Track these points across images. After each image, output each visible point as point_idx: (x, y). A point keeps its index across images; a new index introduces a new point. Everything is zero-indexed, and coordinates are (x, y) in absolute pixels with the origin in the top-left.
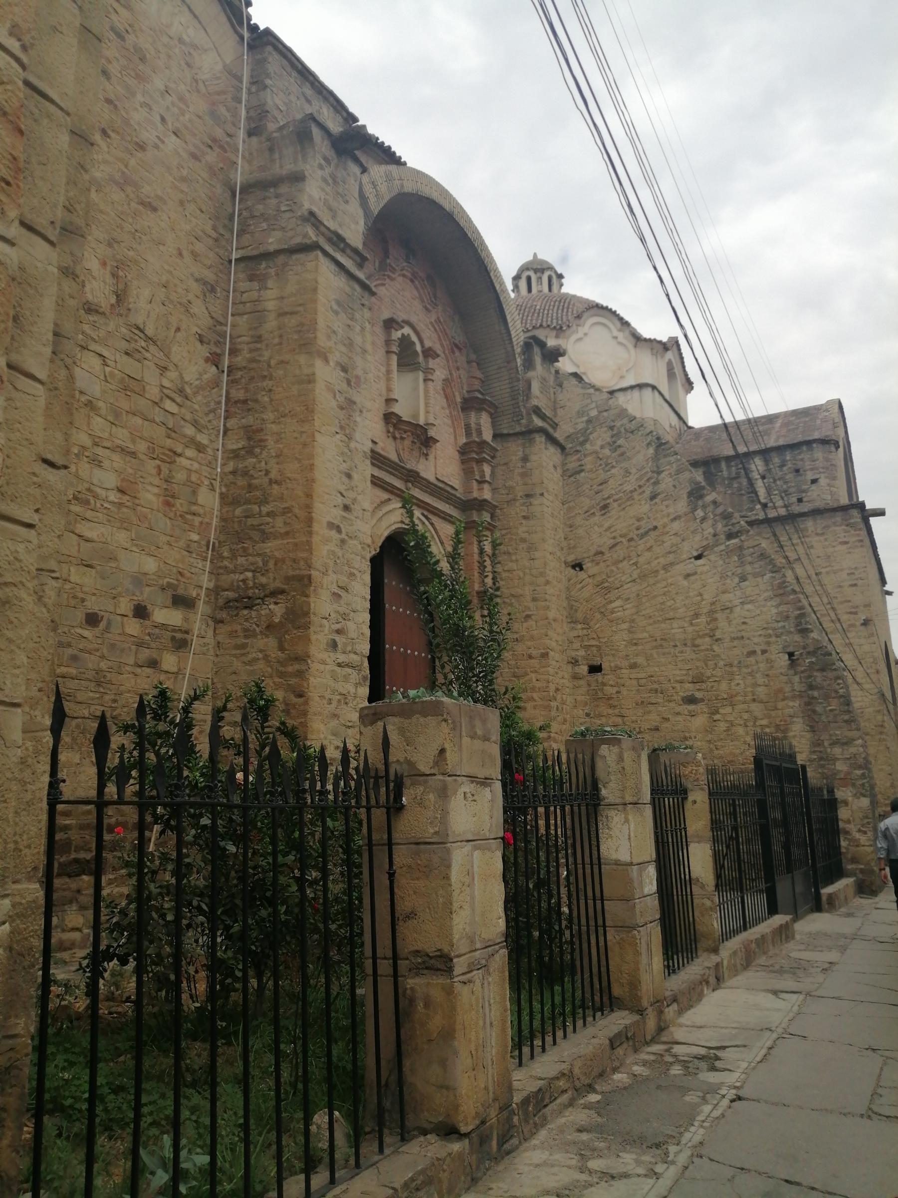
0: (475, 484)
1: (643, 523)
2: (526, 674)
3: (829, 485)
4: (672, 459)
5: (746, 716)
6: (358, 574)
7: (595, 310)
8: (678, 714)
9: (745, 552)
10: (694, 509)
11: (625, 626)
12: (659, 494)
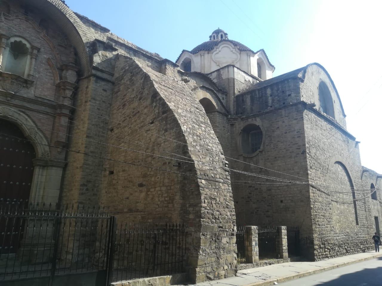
0: (61, 98)
1: (135, 110)
2: (75, 175)
3: (296, 96)
4: (149, 82)
5: (159, 192)
7: (224, 42)
8: (136, 191)
11: (123, 154)
12: (142, 98)
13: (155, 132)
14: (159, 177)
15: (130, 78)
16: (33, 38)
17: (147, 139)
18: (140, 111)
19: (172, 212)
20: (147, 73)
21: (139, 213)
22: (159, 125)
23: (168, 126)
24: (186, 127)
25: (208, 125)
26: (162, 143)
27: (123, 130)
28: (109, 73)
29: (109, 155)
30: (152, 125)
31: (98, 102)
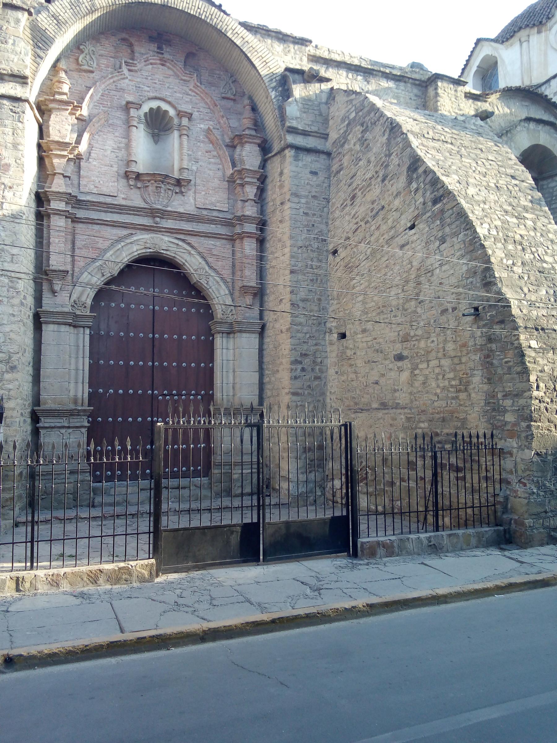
4: (399, 139)
5: (437, 370)
6: (5, 300)
8: (391, 369)
9: (447, 215)
10: (410, 183)
11: (361, 298)
13: (419, 247)
14: (435, 339)
15: (360, 136)
16: (178, 95)
17: (404, 263)
18: (386, 206)
19: (466, 409)
20: (394, 117)
21: (399, 411)
22: (427, 229)
23: (447, 230)
24: (488, 227)
25: (542, 214)
26: (436, 268)
27: (355, 250)
28: (319, 135)
29: (335, 302)
30: (413, 231)
31: (303, 201)
